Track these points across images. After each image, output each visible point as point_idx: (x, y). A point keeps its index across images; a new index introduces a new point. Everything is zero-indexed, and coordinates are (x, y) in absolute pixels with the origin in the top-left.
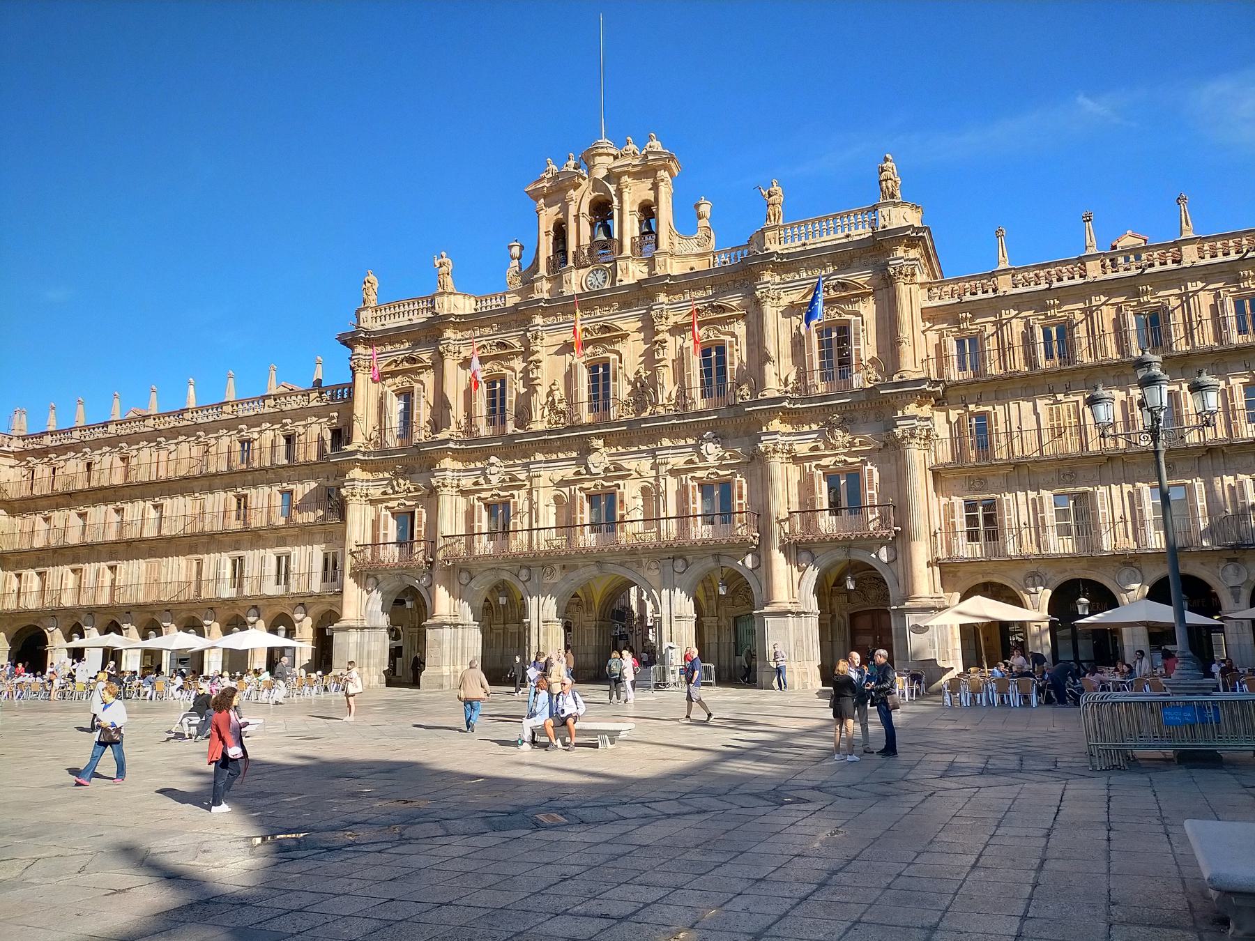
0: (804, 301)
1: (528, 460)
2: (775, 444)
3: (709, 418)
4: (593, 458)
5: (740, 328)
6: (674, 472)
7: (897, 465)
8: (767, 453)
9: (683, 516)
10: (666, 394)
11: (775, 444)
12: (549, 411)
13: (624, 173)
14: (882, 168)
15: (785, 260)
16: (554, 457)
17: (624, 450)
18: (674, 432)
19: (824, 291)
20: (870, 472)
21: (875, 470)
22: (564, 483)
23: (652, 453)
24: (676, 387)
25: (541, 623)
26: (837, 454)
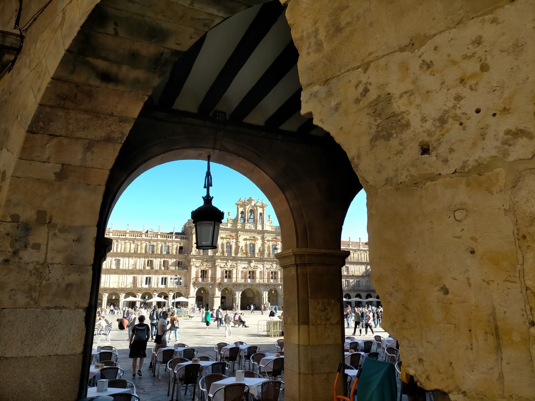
4: (251, 264)
9: (268, 279)
10: (266, 253)
13: (258, 206)
16: (242, 262)
18: (268, 261)
22: (244, 268)
23: (263, 264)
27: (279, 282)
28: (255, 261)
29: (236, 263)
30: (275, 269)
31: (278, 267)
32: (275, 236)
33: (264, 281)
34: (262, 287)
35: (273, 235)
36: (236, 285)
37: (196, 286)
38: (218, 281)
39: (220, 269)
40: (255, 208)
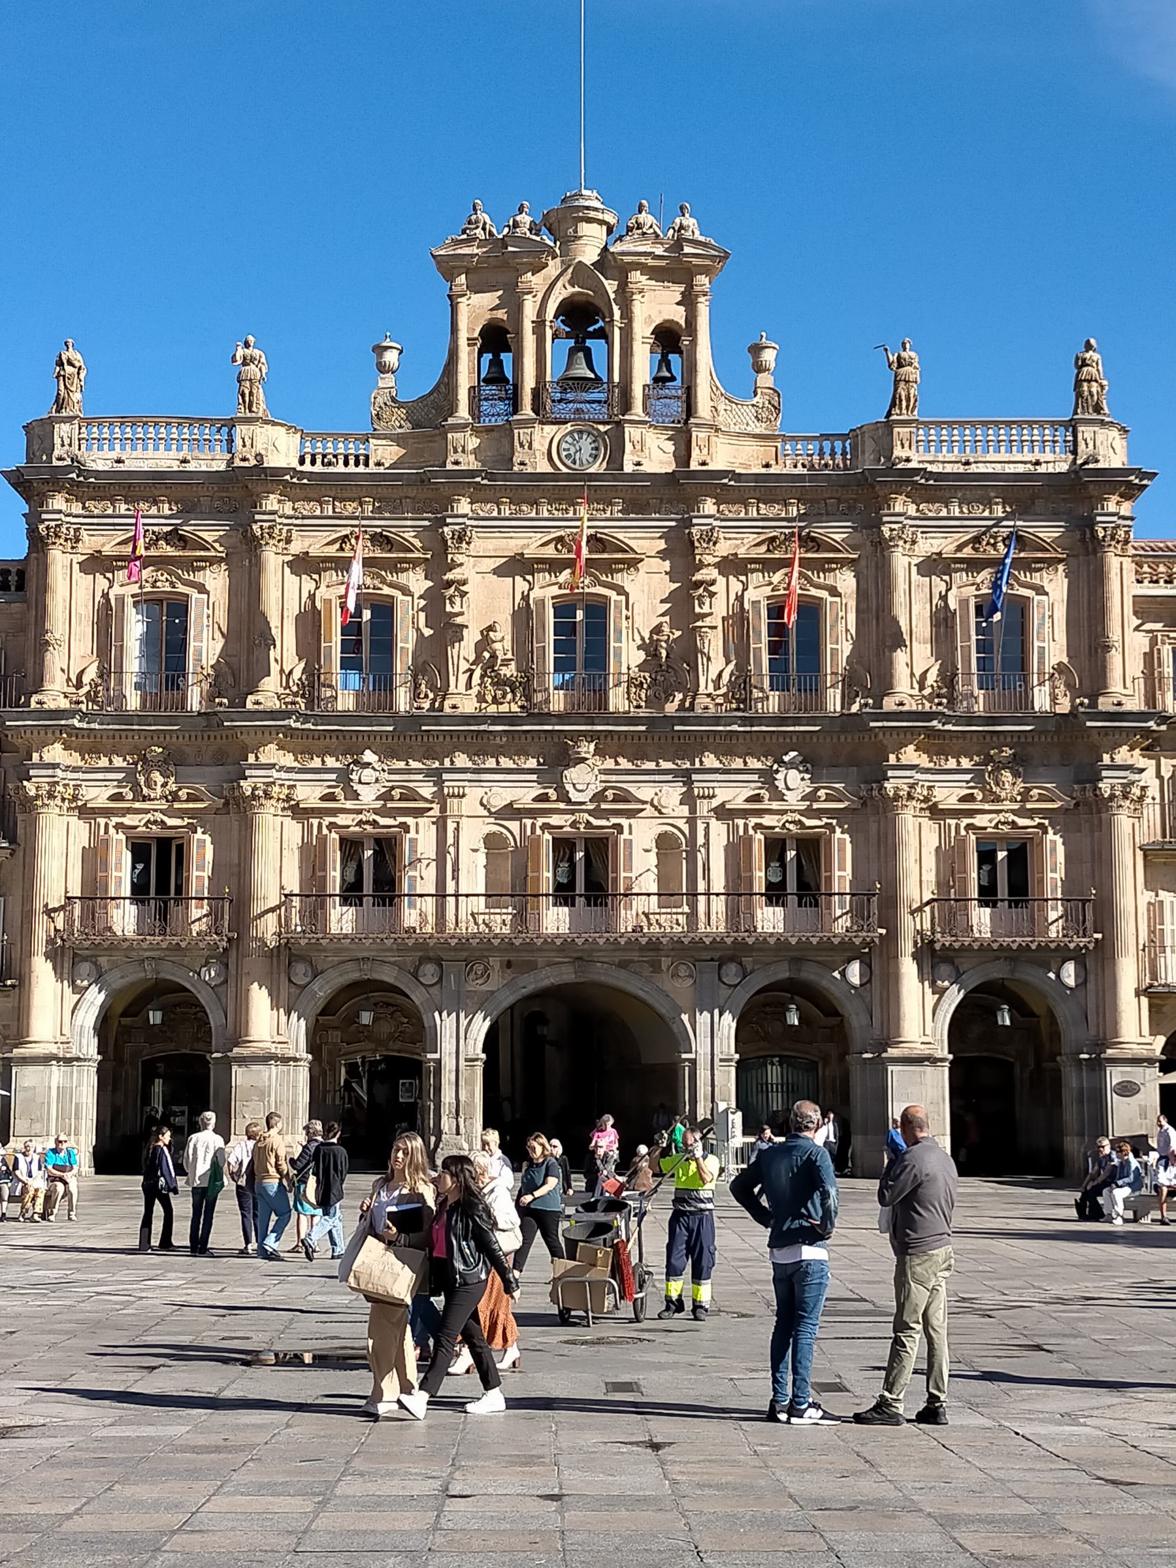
0: (959, 555)
1: (437, 765)
2: (912, 786)
3: (797, 728)
4: (573, 774)
5: (846, 581)
6: (723, 813)
7: (1092, 836)
8: (897, 797)
9: (738, 891)
10: (713, 675)
11: (912, 786)
12: (482, 677)
14: (1084, 360)
15: (931, 482)
16: (491, 763)
17: (630, 766)
18: (726, 745)
19: (988, 544)
20: (1054, 842)
21: (1059, 840)
22: (510, 812)
23: (686, 777)
24: (731, 666)
25: (462, 1063)
26: (1000, 811)
27: (842, 925)
28: (607, 746)
29: (429, 773)
30: (801, 813)
31: (829, 798)
32: (801, 517)
33: (692, 916)
34: (675, 975)
35: (775, 510)
36: (439, 962)
37: (85, 967)
38: (268, 928)
39: (294, 831)
40: (611, 286)
